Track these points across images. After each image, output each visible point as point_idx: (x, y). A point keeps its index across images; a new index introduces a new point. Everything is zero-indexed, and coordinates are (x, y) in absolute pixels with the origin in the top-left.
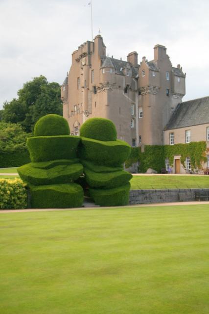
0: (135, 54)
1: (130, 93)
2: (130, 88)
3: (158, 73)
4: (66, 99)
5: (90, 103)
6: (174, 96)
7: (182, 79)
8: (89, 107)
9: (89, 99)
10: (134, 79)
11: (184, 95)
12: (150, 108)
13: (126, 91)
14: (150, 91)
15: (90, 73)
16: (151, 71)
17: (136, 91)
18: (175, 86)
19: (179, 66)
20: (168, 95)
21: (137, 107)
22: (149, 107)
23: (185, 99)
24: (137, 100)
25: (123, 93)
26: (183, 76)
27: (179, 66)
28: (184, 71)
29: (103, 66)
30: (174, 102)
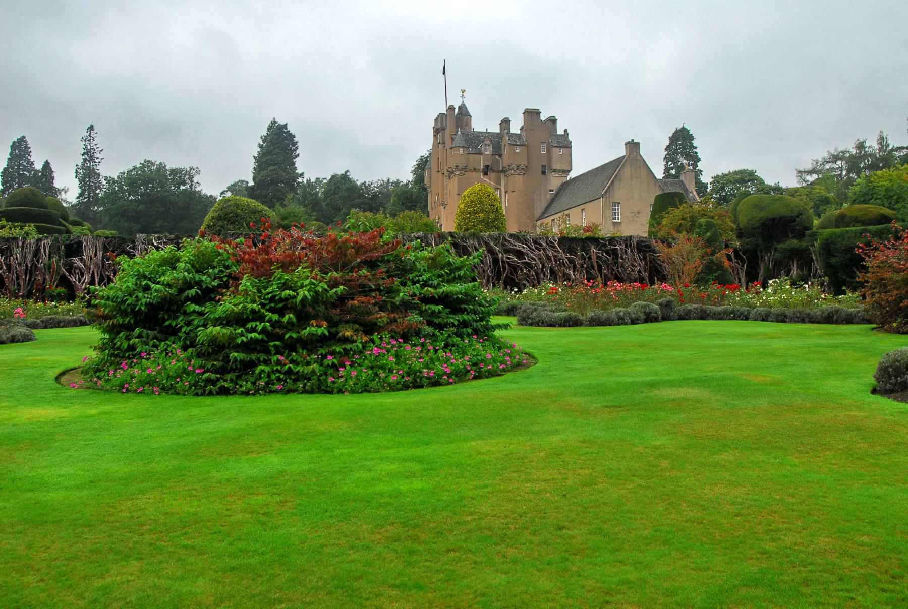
0: (505, 121)
1: (493, 175)
2: (491, 169)
3: (524, 147)
4: (430, 187)
5: (445, 191)
6: (553, 174)
7: (566, 150)
8: (445, 196)
9: (445, 186)
10: (497, 157)
11: (569, 171)
12: (514, 193)
13: (486, 174)
14: (512, 172)
15: (445, 154)
16: (511, 147)
17: (503, 171)
18: (554, 161)
19: (566, 131)
20: (544, 173)
21: (503, 193)
22: (513, 191)
23: (573, 175)
24: (503, 183)
25: (482, 177)
26: (568, 146)
27: (566, 131)
28: (571, 138)
29: (456, 143)
30: (555, 182)
